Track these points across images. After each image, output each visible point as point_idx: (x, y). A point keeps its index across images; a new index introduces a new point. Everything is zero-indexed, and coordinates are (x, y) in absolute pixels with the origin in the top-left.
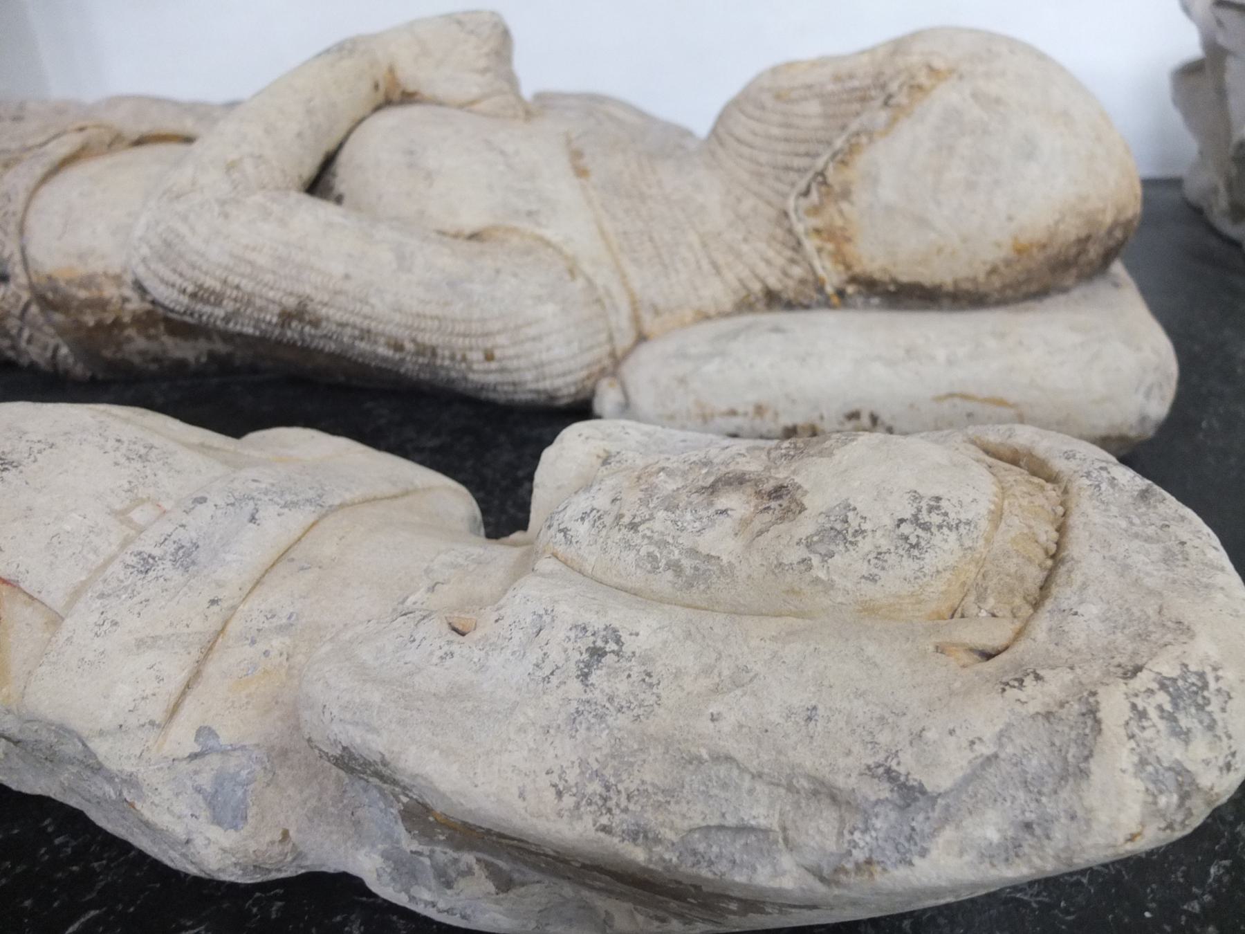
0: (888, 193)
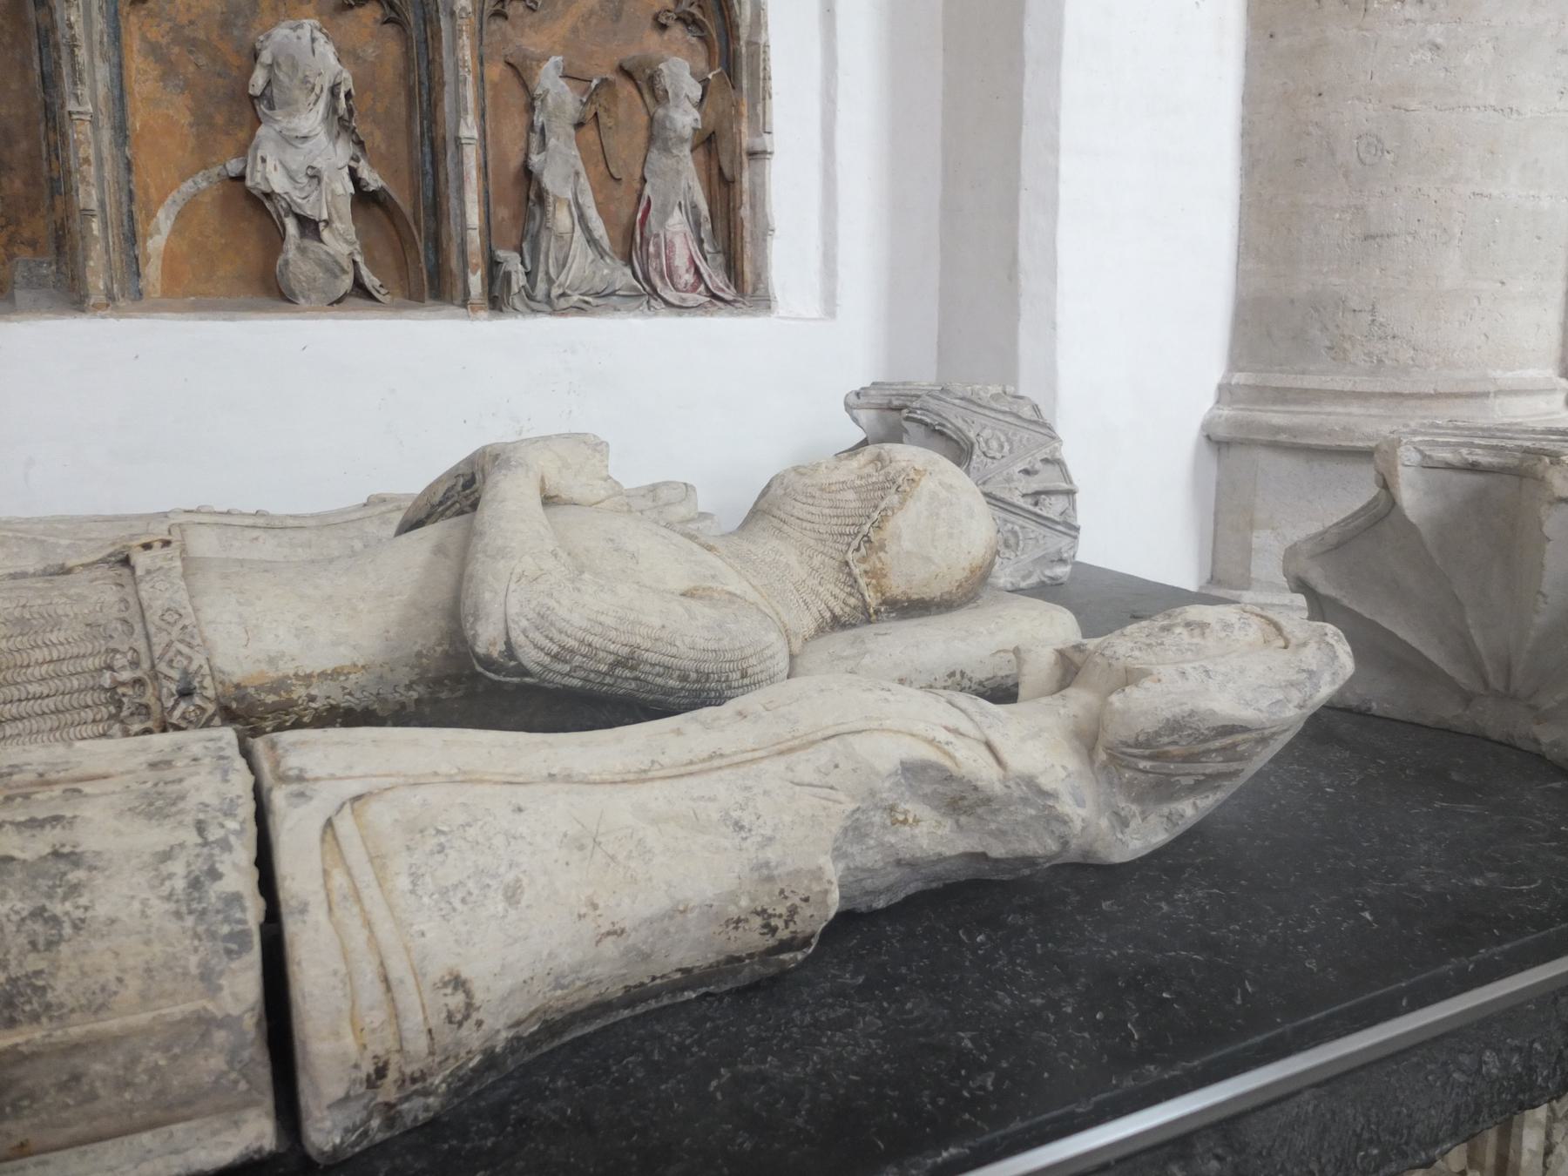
0: (907, 544)
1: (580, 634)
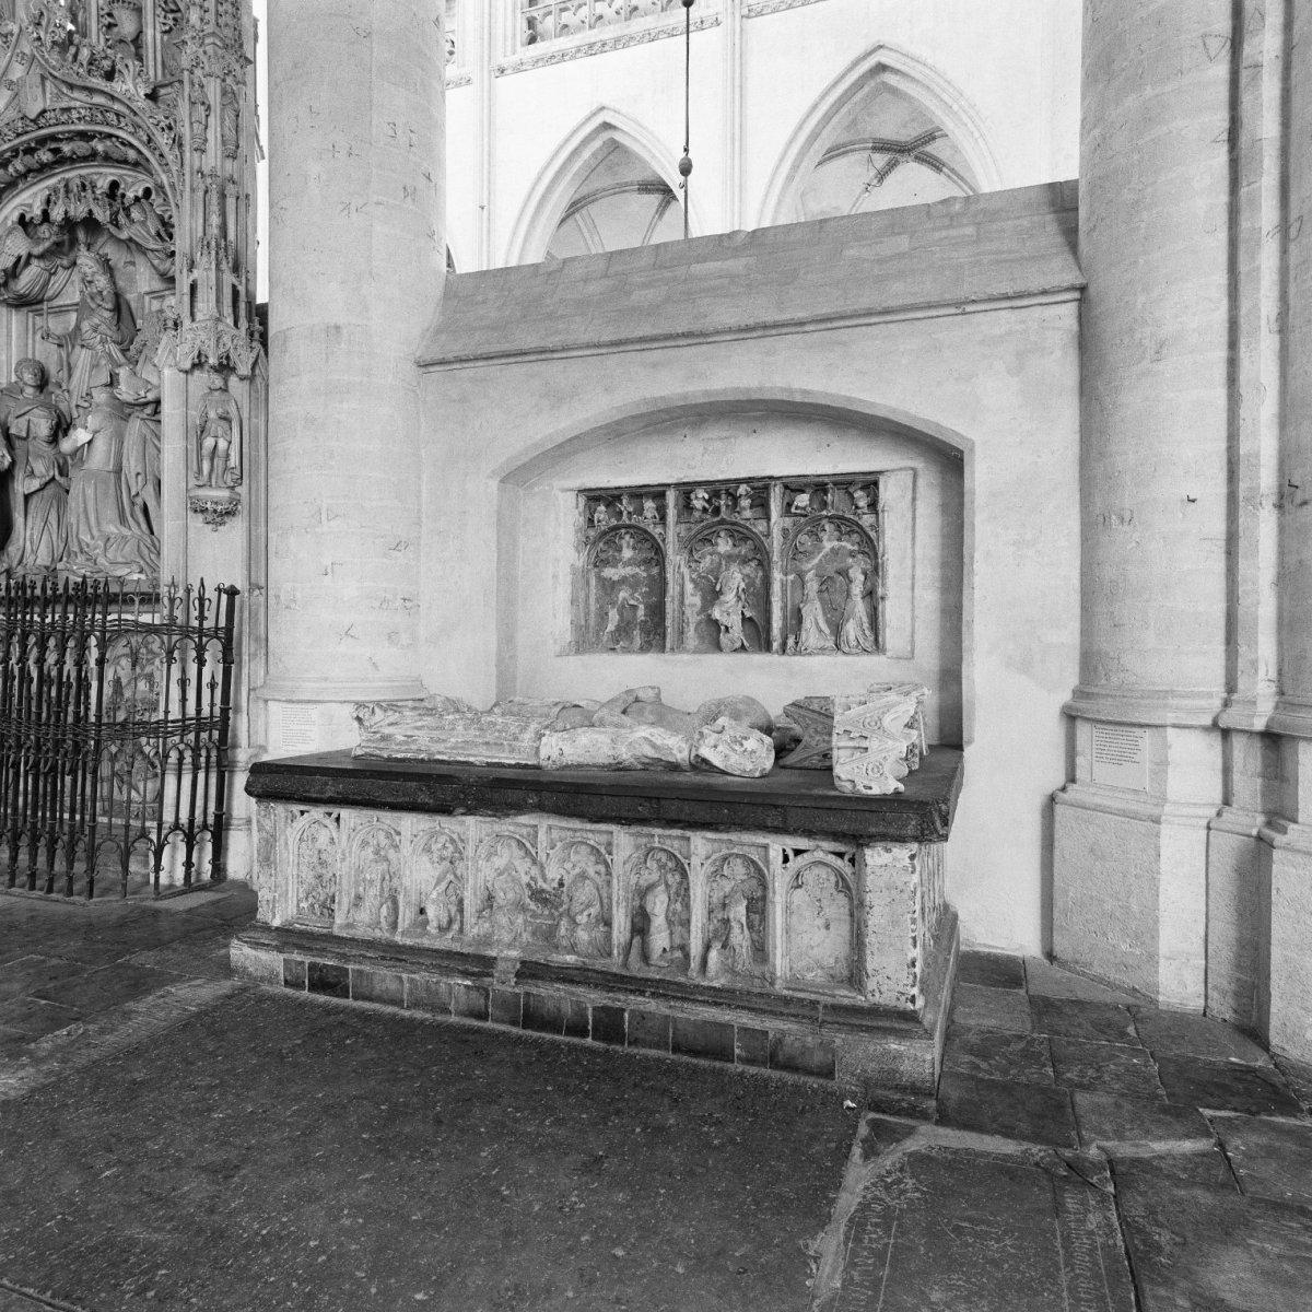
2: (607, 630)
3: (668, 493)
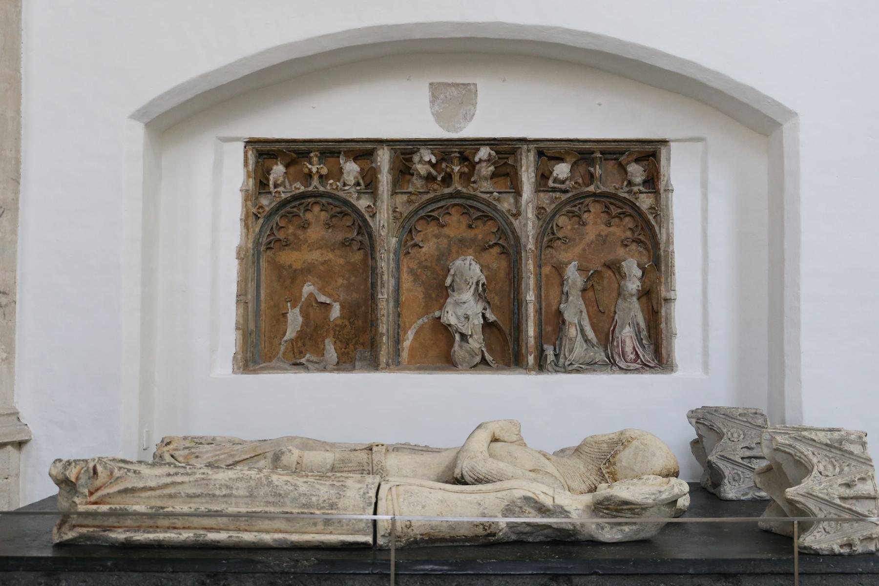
0: (624, 464)
1: (484, 475)
2: (285, 338)
3: (380, 152)
